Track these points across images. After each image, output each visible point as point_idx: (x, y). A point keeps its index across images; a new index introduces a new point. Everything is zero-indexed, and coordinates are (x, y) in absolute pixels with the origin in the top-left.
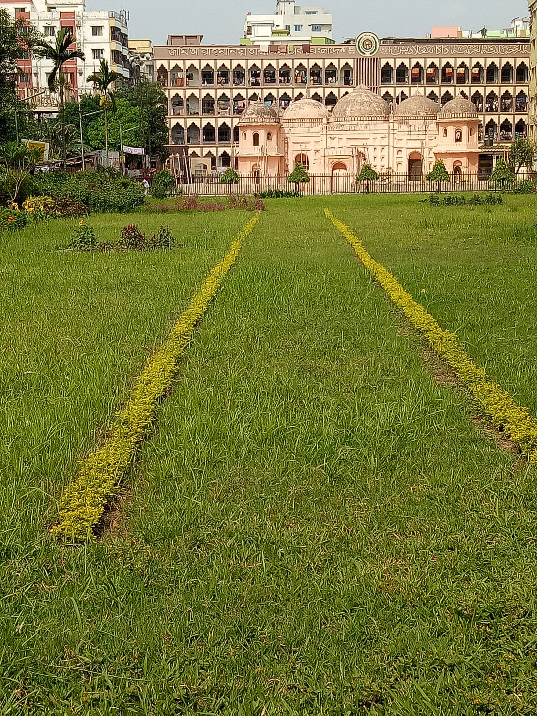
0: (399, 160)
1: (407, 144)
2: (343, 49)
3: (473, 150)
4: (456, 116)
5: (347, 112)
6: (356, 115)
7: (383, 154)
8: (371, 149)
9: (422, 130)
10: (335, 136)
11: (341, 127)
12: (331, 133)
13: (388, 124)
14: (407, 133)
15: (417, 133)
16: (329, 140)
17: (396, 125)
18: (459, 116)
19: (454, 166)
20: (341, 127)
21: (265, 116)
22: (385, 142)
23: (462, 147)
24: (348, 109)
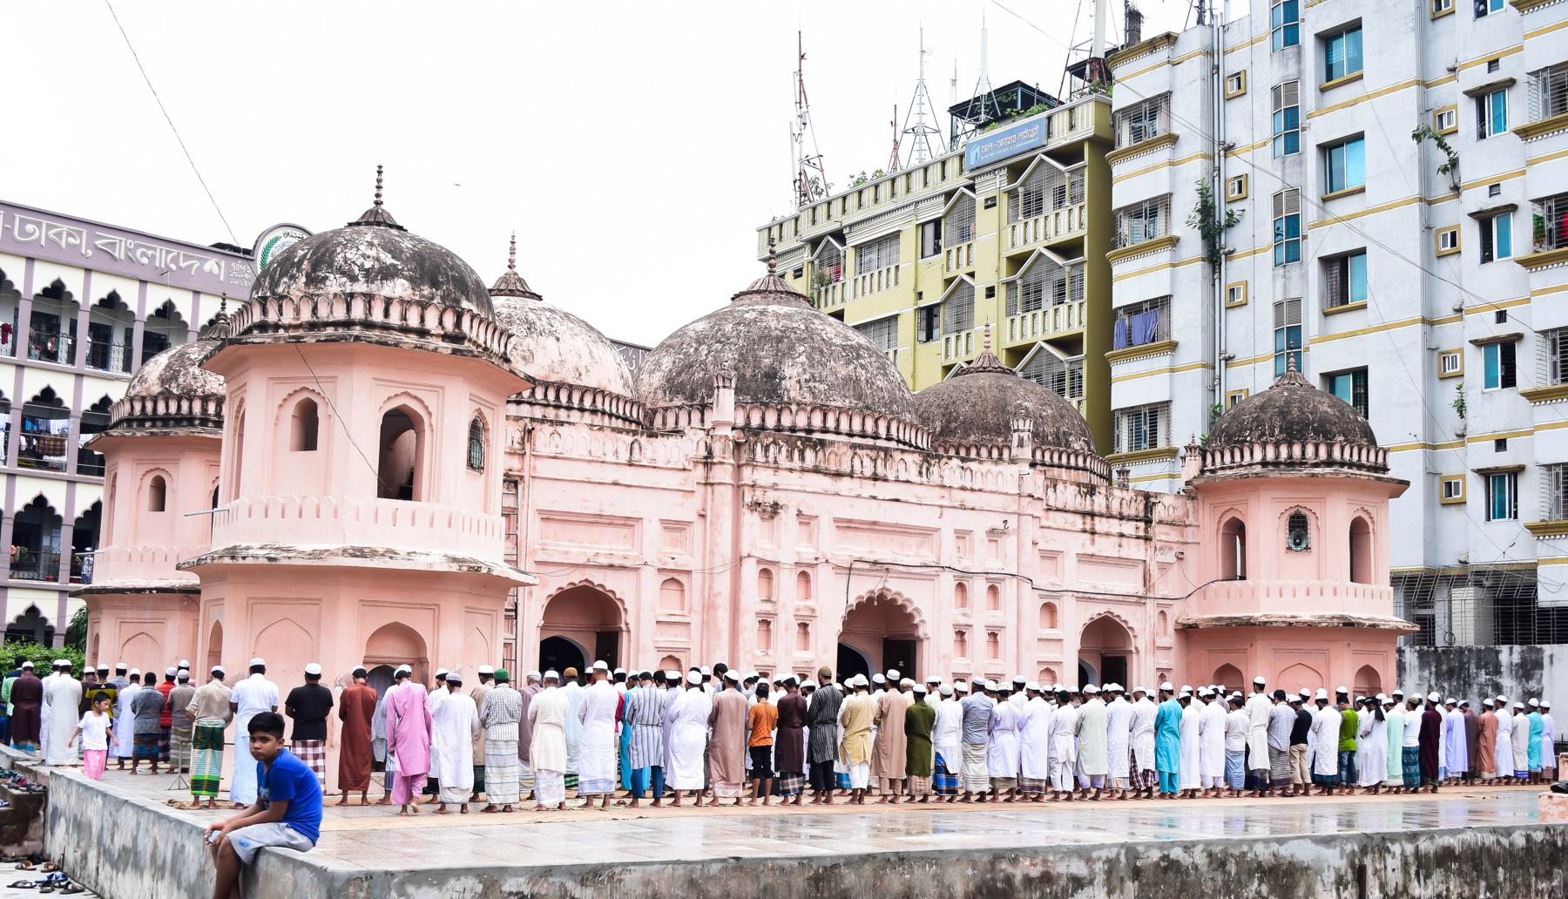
0: (1051, 654)
2: (212, 264)
4: (1355, 458)
6: (839, 404)
7: (996, 618)
8: (948, 581)
9: (1133, 513)
10: (781, 497)
11: (809, 454)
12: (764, 477)
13: (1014, 469)
14: (1078, 520)
15: (1115, 526)
16: (751, 520)
18: (1364, 460)
20: (809, 454)
21: (465, 304)
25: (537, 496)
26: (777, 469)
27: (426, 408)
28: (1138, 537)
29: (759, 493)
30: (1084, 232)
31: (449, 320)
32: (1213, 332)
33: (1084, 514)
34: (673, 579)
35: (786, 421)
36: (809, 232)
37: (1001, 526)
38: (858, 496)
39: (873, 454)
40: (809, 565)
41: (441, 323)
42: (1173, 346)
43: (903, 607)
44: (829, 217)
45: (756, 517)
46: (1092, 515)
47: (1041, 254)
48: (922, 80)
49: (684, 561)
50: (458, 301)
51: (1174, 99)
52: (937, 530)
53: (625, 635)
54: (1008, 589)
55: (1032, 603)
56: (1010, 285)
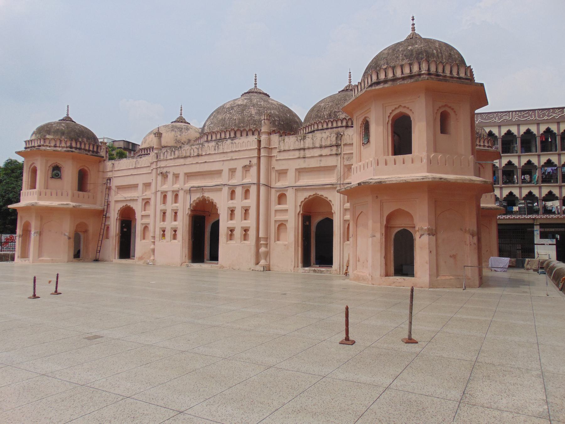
0: (280, 217)
1: (297, 179)
3: (451, 177)
5: (206, 127)
7: (246, 203)
8: (226, 190)
9: (328, 143)
12: (162, 164)
14: (297, 154)
15: (317, 152)
16: (160, 178)
17: (275, 138)
18: (399, 74)
19: (388, 228)
20: (177, 152)
21: (48, 136)
22: (251, 178)
23: (413, 169)
25: (115, 183)
26: (167, 160)
28: (330, 155)
29: (162, 169)
33: (300, 149)
34: (147, 202)
37: (248, 163)
38: (192, 164)
39: (197, 146)
40: (178, 191)
43: (213, 203)
46: (304, 149)
49: (148, 194)
50: (45, 136)
52: (222, 170)
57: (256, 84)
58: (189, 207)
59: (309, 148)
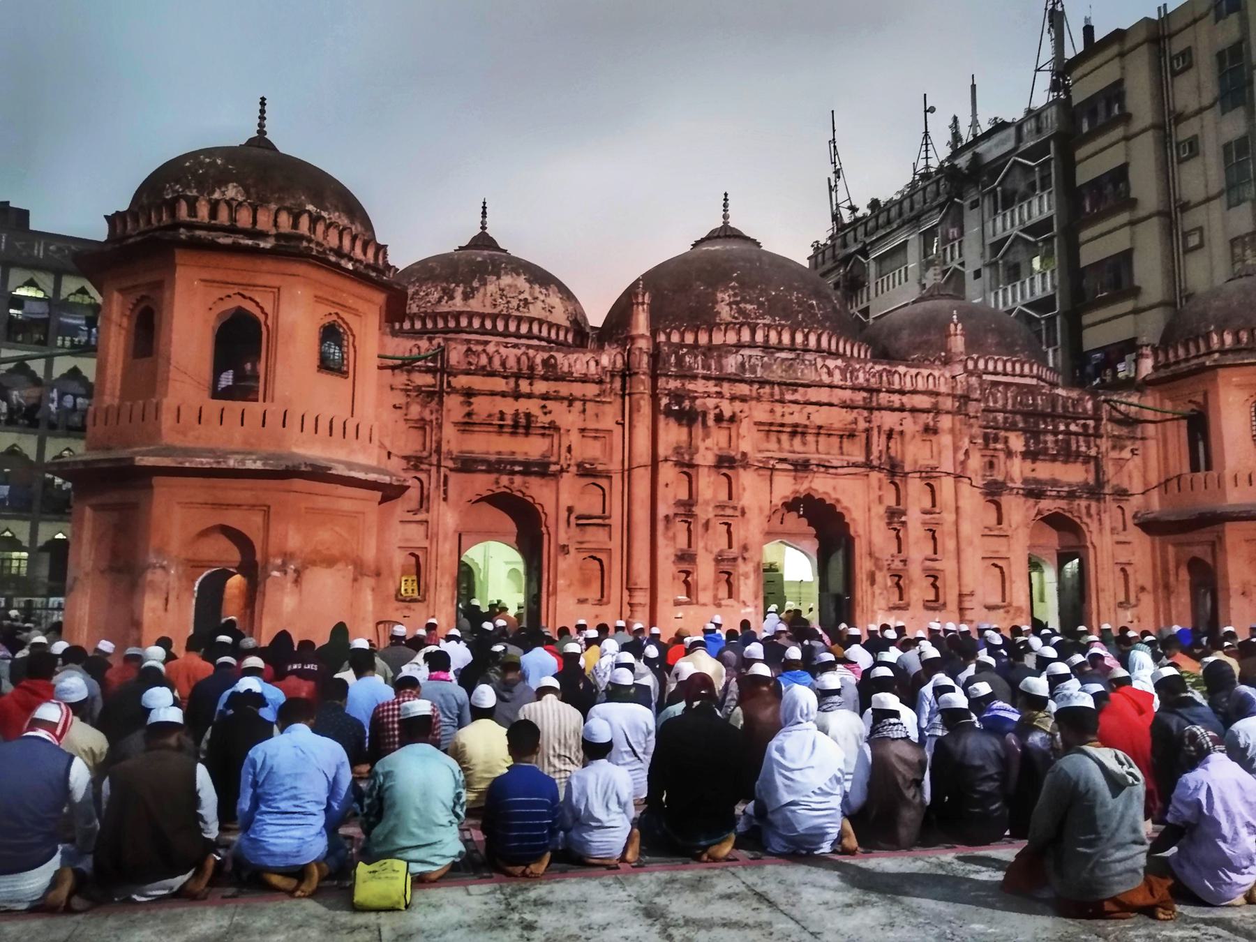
24: (720, 296)
26: (695, 377)
27: (262, 309)
30: (1053, 211)
31: (285, 220)
32: (1173, 272)
35: (718, 339)
36: (841, 253)
41: (275, 221)
42: (1135, 292)
44: (856, 240)
45: (673, 424)
47: (1017, 237)
48: (926, 133)
51: (1128, 85)
53: (546, 537)
54: (946, 486)
55: (971, 499)
56: (993, 265)
57: (725, 217)
58: (767, 512)
59: (1043, 416)
